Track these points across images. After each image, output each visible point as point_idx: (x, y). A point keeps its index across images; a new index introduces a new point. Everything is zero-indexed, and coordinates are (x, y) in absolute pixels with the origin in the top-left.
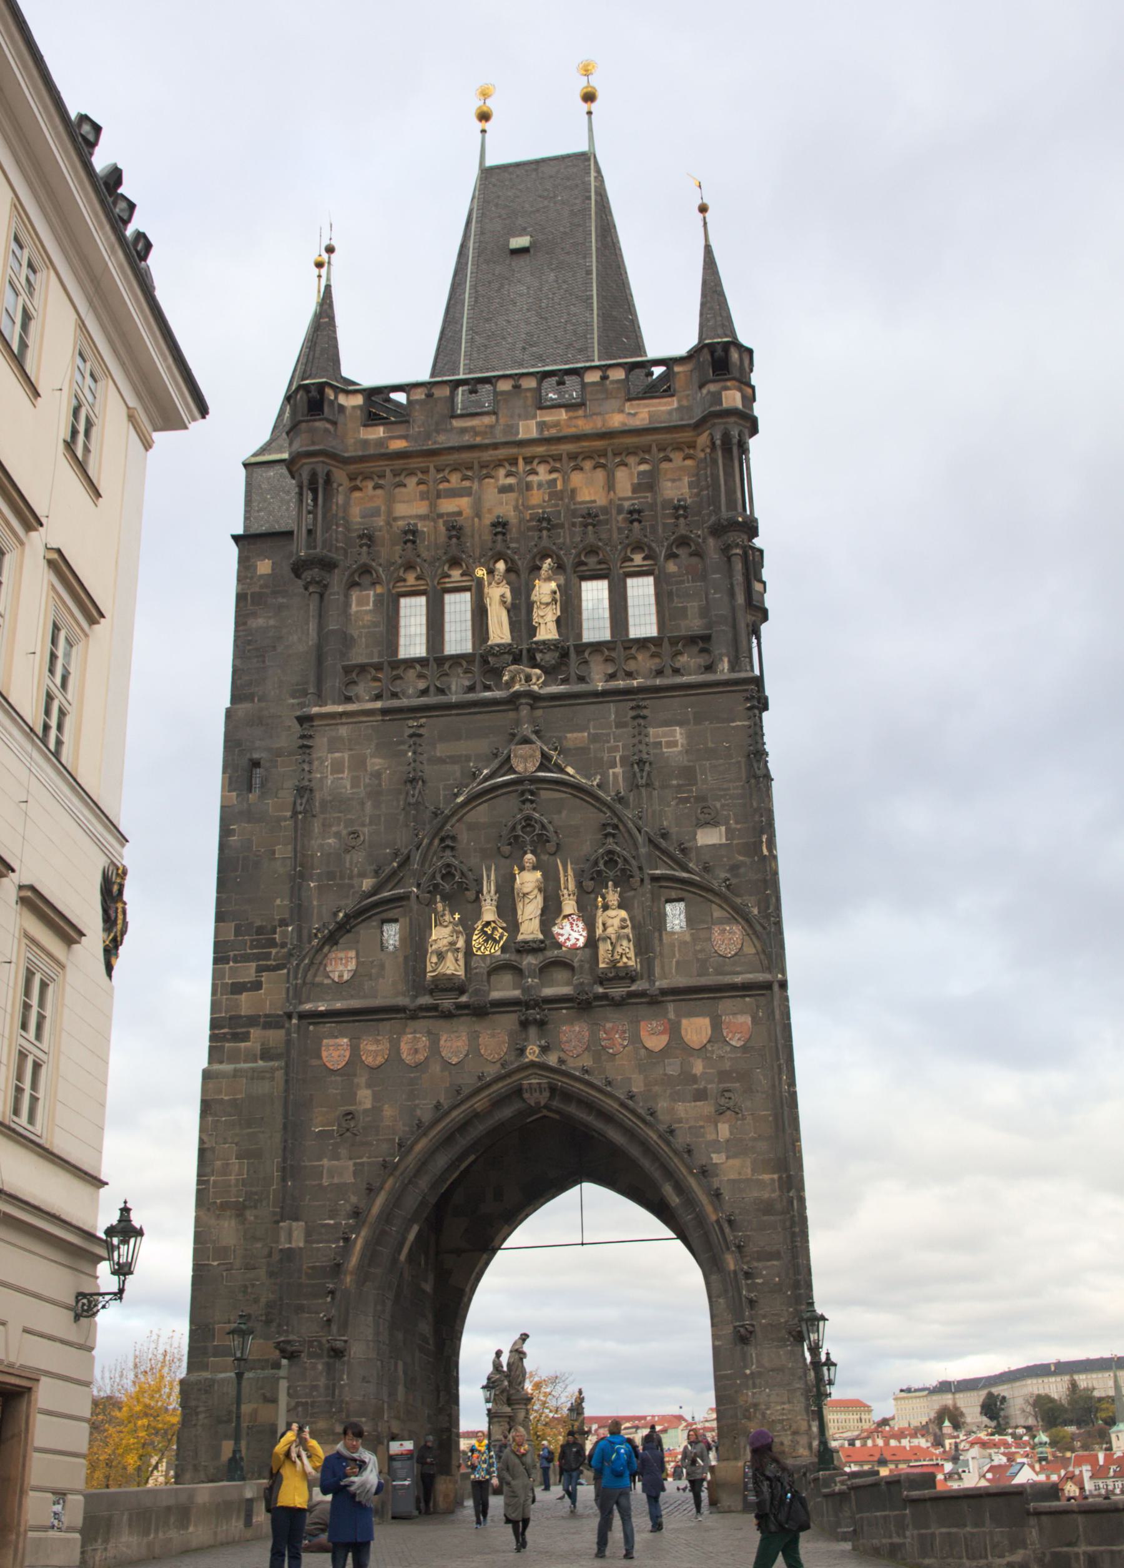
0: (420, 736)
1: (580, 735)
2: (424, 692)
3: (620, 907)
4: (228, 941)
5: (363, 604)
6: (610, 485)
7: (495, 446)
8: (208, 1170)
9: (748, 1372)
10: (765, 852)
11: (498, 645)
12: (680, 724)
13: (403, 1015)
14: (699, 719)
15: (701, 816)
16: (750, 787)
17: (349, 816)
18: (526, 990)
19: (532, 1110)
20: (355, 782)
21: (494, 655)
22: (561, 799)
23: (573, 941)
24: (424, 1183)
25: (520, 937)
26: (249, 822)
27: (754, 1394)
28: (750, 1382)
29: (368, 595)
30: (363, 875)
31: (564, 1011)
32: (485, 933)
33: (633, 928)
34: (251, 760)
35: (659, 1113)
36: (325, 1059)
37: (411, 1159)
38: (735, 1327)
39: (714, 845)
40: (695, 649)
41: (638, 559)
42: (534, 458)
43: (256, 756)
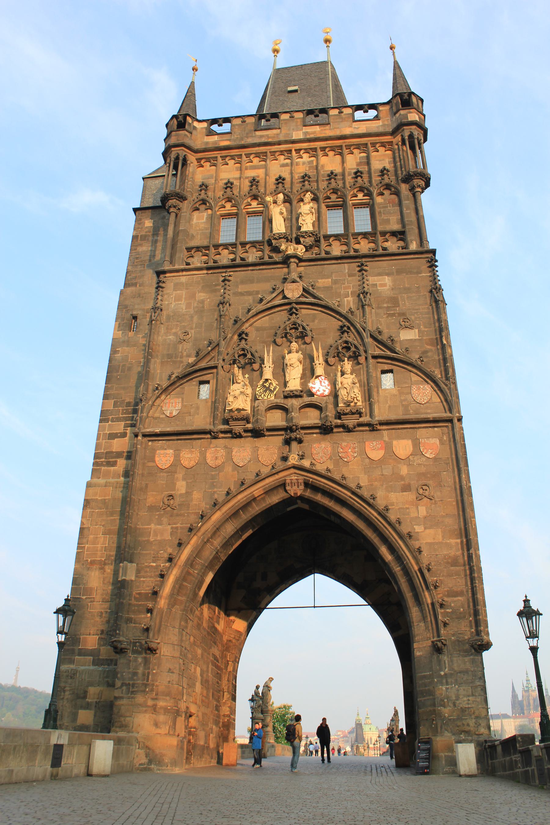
0: (229, 281)
1: (326, 280)
2: (234, 260)
3: (351, 374)
4: (109, 410)
5: (199, 220)
6: (343, 162)
7: (279, 143)
8: (85, 540)
9: (442, 673)
10: (445, 342)
11: (278, 234)
12: (388, 274)
13: (209, 436)
14: (399, 272)
15: (403, 323)
16: (432, 308)
17: (183, 324)
18: (289, 420)
19: (291, 500)
20: (188, 306)
21: (275, 239)
22: (314, 314)
23: (321, 392)
24: (217, 542)
25: (287, 389)
26: (127, 346)
27: (447, 689)
28: (444, 681)
29: (203, 216)
30: (189, 356)
31: (315, 435)
32: (265, 386)
33: (360, 386)
34: (132, 315)
35: (378, 499)
36: (157, 462)
37: (209, 525)
38: (433, 642)
39: (411, 340)
40: (395, 239)
41: (360, 196)
42: (300, 150)
43: (135, 313)
